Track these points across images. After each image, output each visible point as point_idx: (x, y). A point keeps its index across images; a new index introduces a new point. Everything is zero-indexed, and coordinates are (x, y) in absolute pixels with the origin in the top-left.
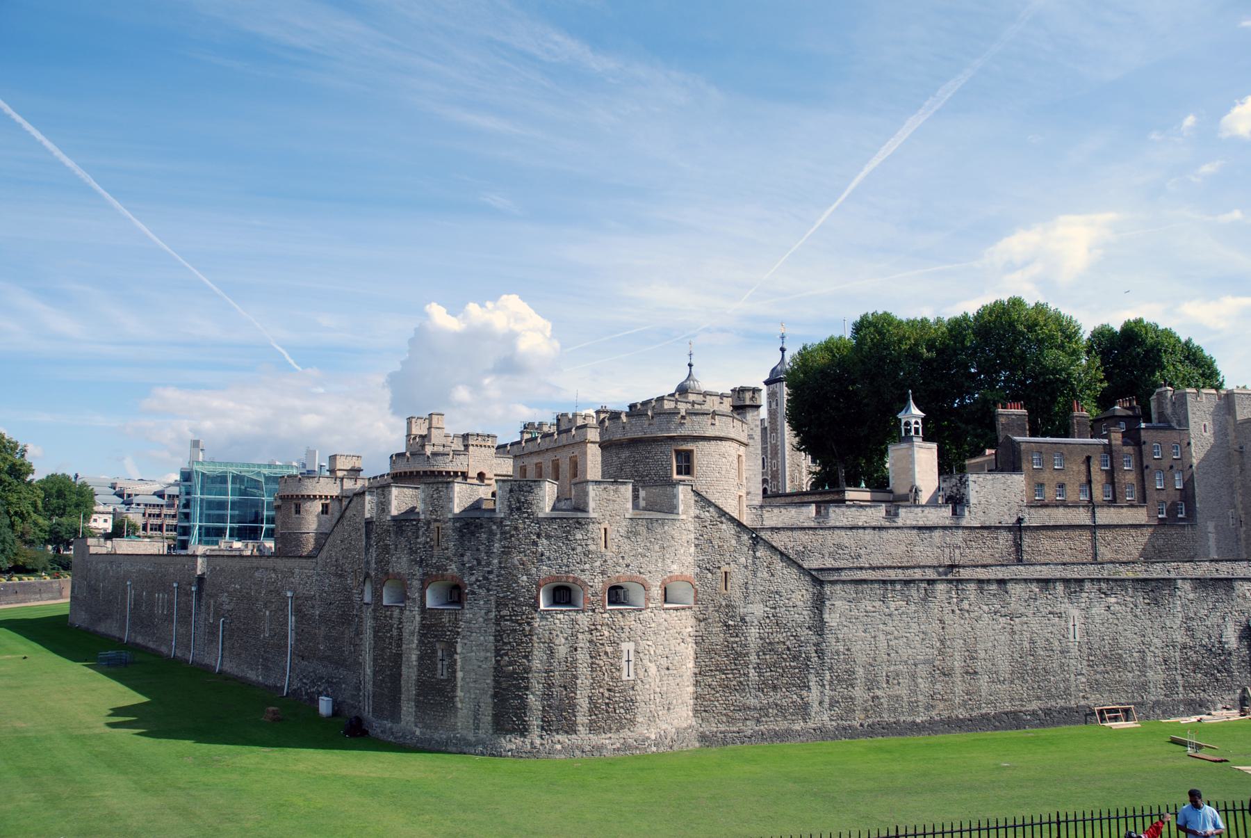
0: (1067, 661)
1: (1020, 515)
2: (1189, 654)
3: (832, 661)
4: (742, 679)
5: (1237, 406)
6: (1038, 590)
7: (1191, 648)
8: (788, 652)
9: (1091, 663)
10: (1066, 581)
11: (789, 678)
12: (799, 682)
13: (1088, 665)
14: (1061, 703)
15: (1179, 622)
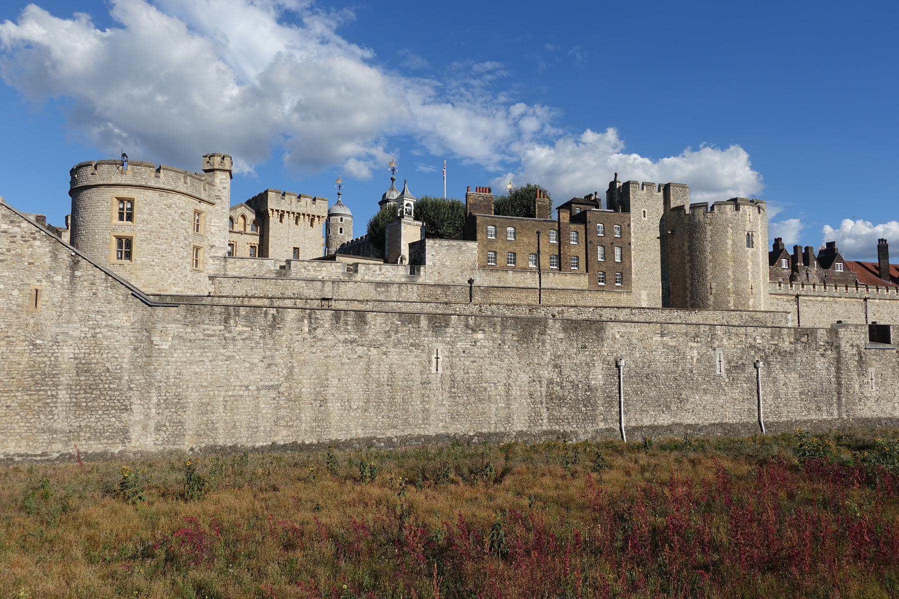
0: (428, 392)
1: (472, 276)
2: (555, 389)
3: (160, 384)
4: (48, 401)
5: (671, 196)
6: (400, 323)
7: (557, 383)
8: (108, 374)
9: (453, 395)
10: (432, 317)
11: (108, 401)
12: (118, 404)
13: (450, 397)
14: (417, 432)
15: (547, 359)
